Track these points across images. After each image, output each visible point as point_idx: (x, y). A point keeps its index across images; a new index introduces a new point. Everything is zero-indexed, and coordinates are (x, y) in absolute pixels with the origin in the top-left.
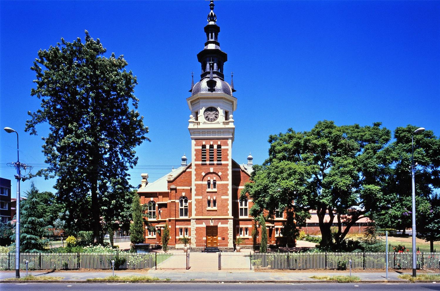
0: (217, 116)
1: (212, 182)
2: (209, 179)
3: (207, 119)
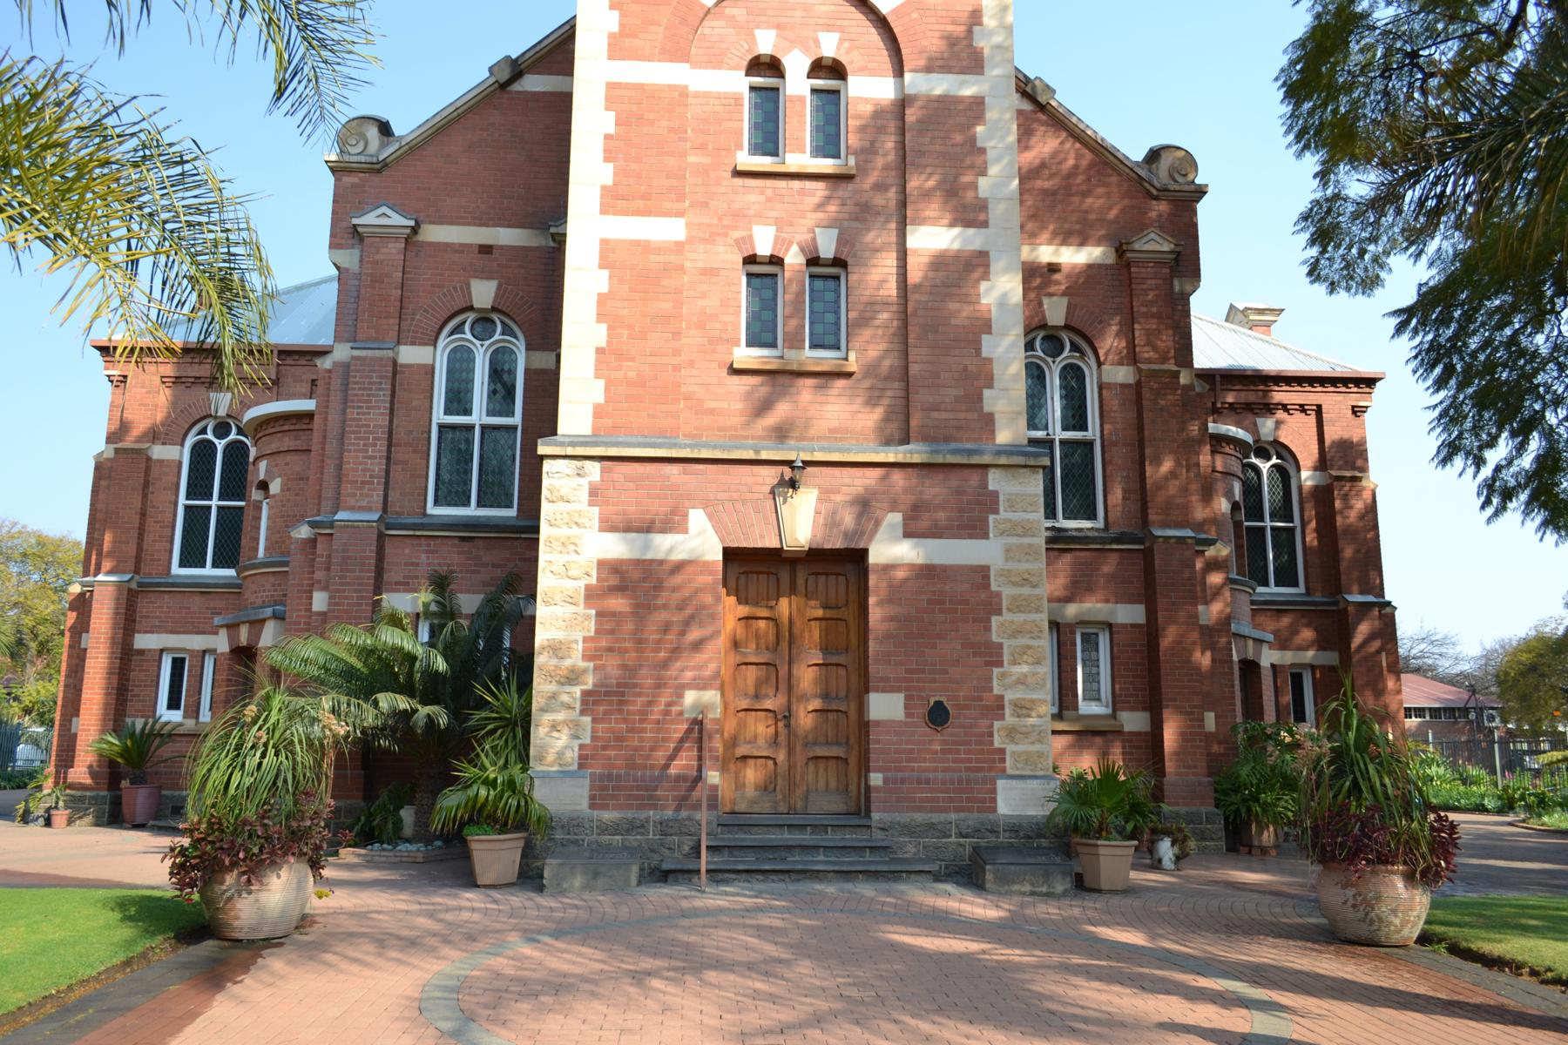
1: (798, 83)
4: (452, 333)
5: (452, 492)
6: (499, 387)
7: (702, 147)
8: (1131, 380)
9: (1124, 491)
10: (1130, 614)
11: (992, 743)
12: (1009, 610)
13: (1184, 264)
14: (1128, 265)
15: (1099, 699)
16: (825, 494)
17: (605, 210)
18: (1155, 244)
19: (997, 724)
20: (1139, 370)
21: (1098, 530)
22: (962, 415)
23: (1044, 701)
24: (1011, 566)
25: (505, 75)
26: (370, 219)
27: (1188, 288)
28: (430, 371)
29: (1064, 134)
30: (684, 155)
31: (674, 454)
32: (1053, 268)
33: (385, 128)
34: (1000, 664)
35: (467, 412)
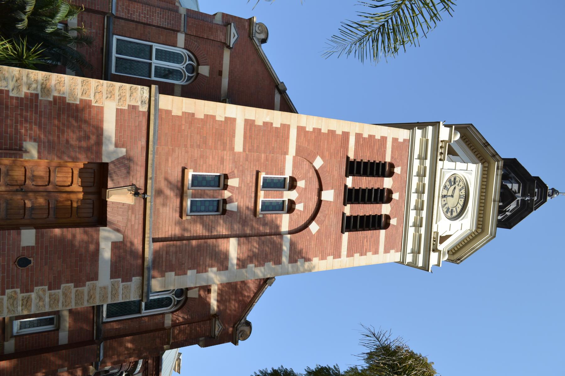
0: (449, 214)
1: (288, 195)
3: (448, 183)
4: (189, 56)
5: (122, 47)
6: (167, 72)
7: (267, 160)
8: (166, 326)
9: (119, 329)
10: (63, 337)
11: (8, 288)
12: (77, 291)
13: (209, 340)
14: (210, 319)
15: (21, 329)
16: (131, 208)
17: (246, 121)
18: (218, 329)
19: (18, 290)
20: (170, 329)
21: (102, 319)
22: (164, 264)
23: (30, 310)
24: (98, 290)
25: (280, 88)
26: (233, 30)
27: (201, 343)
28: (175, 45)
29: (255, 291)
30: (265, 152)
31: (151, 143)
32: (209, 291)
33: (264, 41)
34: (50, 289)
35: (156, 59)
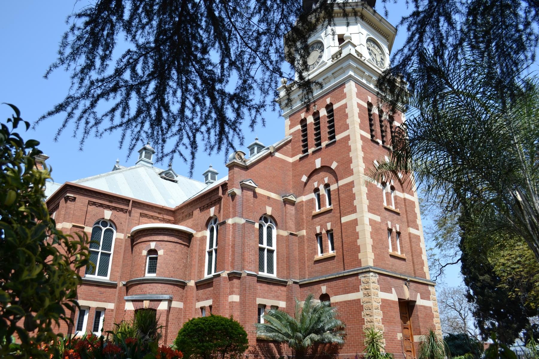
1: (323, 191)
2: (316, 186)
